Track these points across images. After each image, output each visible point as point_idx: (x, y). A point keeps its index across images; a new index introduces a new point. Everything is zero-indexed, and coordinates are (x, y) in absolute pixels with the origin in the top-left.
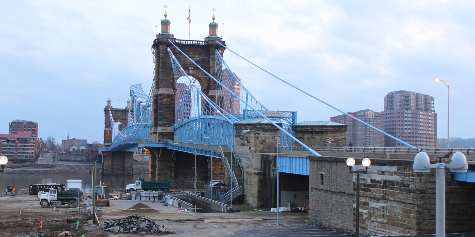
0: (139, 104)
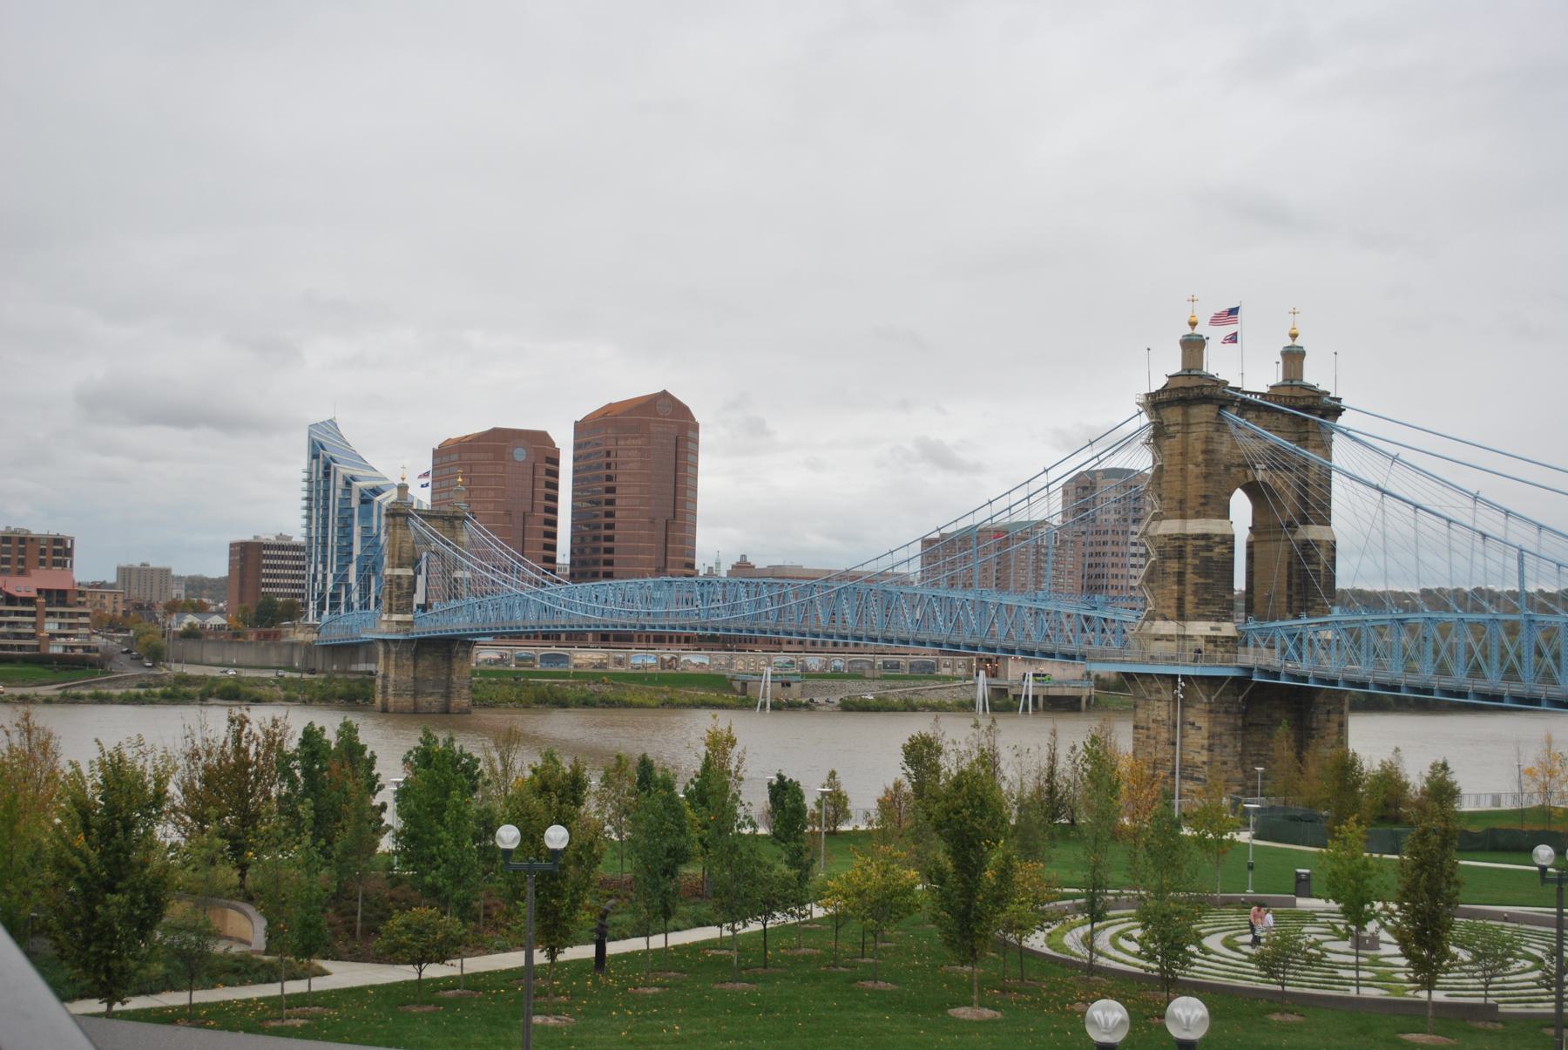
0: (348, 484)
